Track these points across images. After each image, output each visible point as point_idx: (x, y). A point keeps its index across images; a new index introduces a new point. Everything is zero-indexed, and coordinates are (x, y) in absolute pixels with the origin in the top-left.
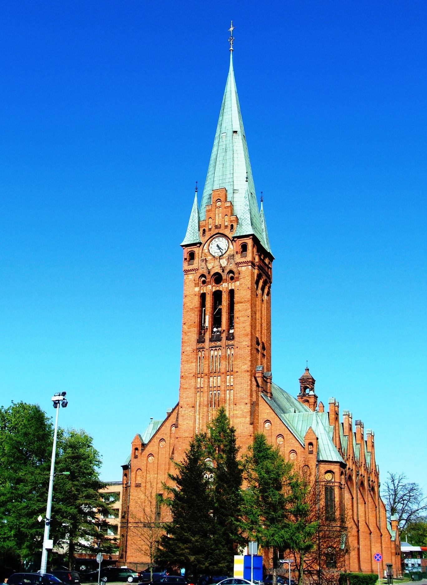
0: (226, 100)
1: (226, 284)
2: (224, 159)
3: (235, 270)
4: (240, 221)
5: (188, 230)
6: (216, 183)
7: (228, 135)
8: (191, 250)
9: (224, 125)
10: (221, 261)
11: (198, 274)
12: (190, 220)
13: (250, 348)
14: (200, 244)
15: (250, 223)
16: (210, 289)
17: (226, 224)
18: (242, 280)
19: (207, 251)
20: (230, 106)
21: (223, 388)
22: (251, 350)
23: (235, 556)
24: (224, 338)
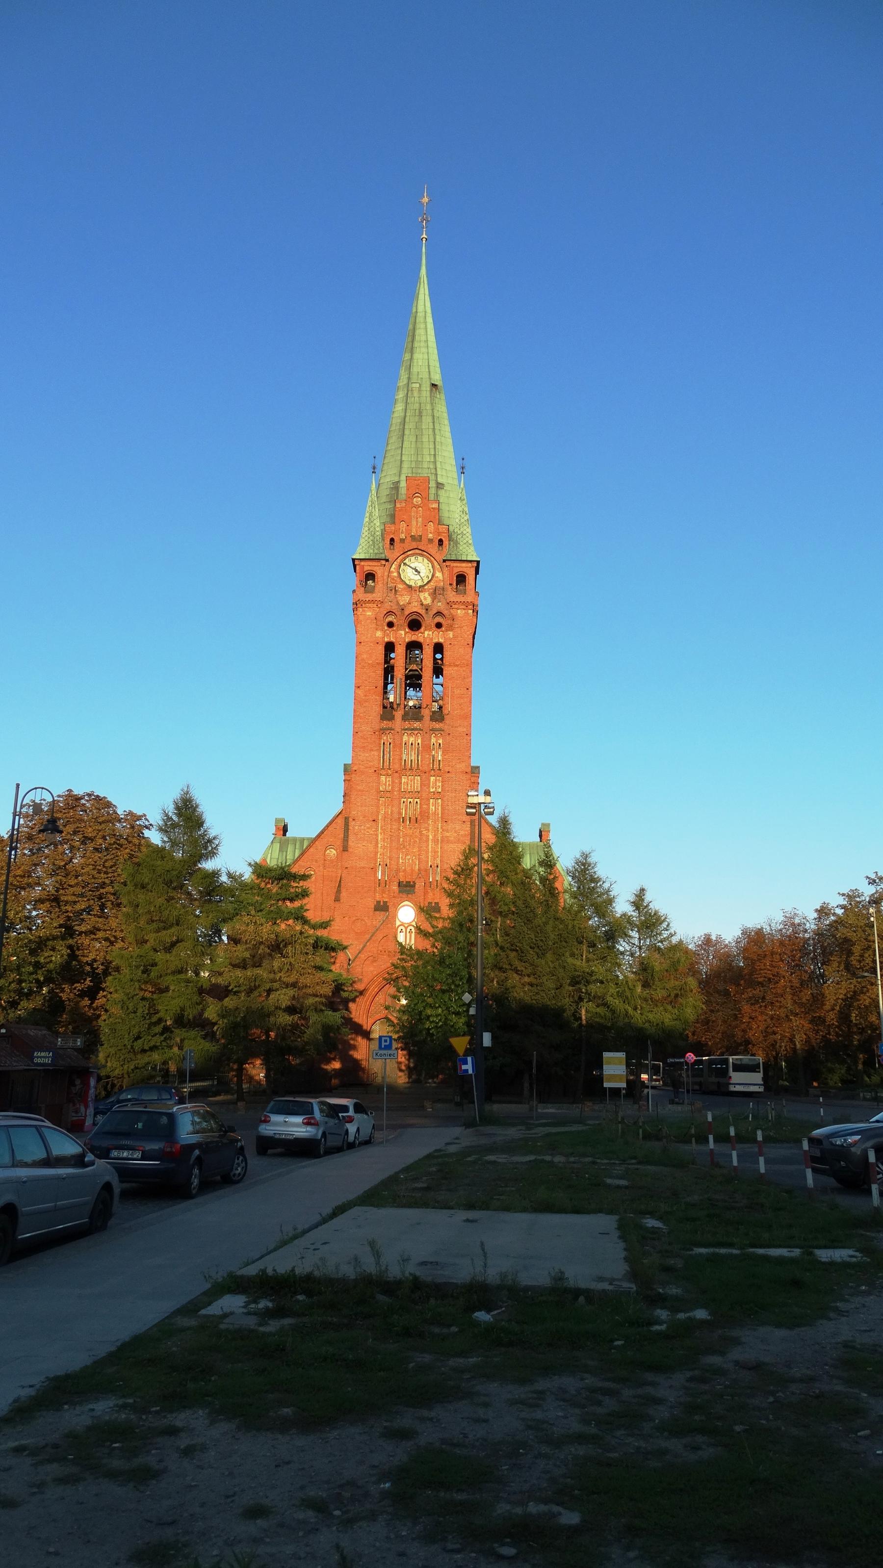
0: (418, 326)
2: (418, 427)
3: (445, 612)
4: (454, 536)
6: (405, 465)
7: (423, 388)
8: (369, 568)
9: (415, 370)
14: (387, 560)
17: (430, 536)
18: (458, 631)
19: (395, 574)
20: (423, 338)
21: (424, 795)
24: (427, 718)
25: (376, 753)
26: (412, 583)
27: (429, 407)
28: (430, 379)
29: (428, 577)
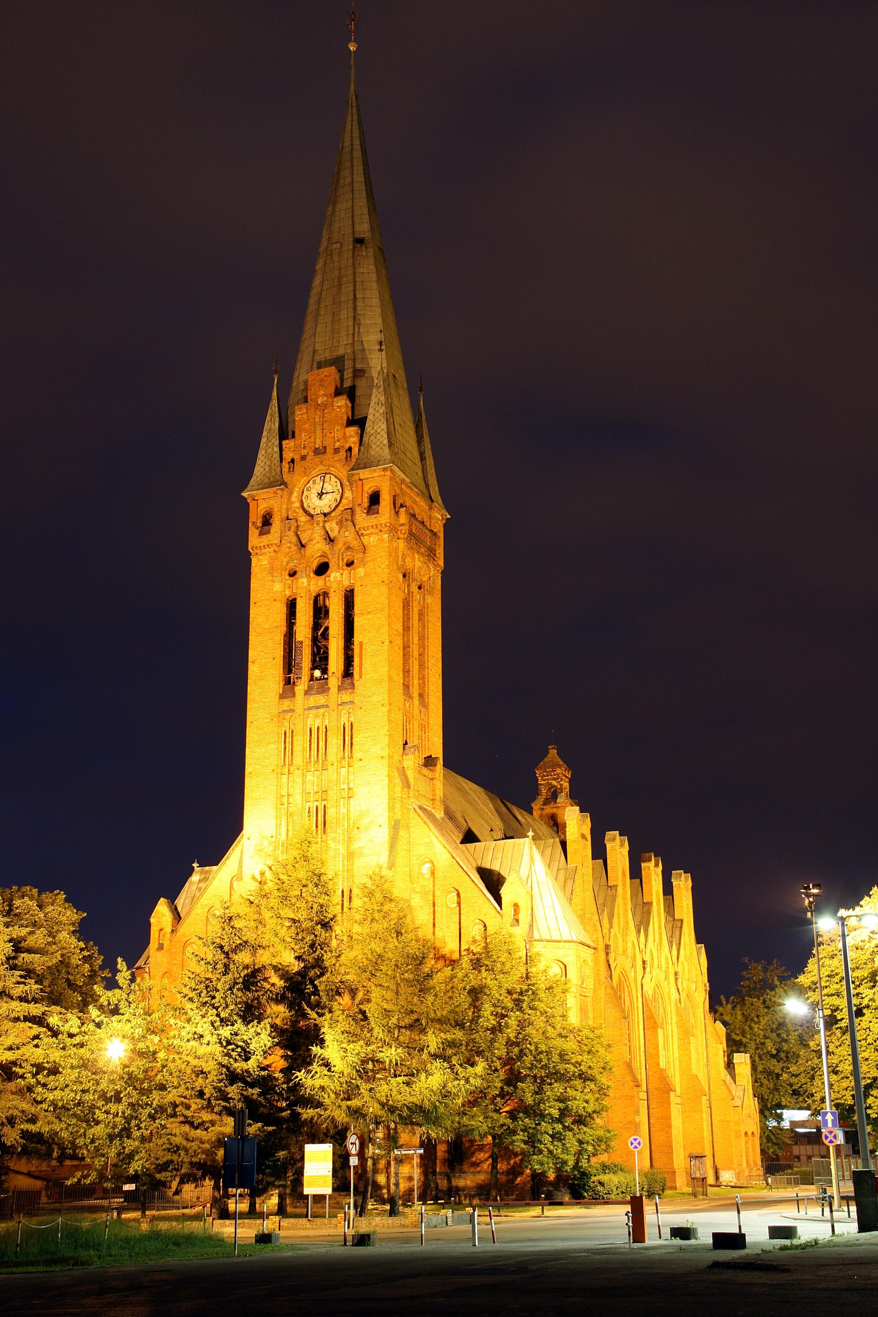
1: (338, 574)
3: (355, 543)
5: (259, 462)
10: (327, 525)
12: (264, 440)
13: (386, 709)
15: (386, 442)
16: (307, 586)
19: (297, 505)
20: (348, 180)
22: (389, 711)
23: (306, 1145)
25: (273, 746)
27: (350, 271)
28: (353, 232)
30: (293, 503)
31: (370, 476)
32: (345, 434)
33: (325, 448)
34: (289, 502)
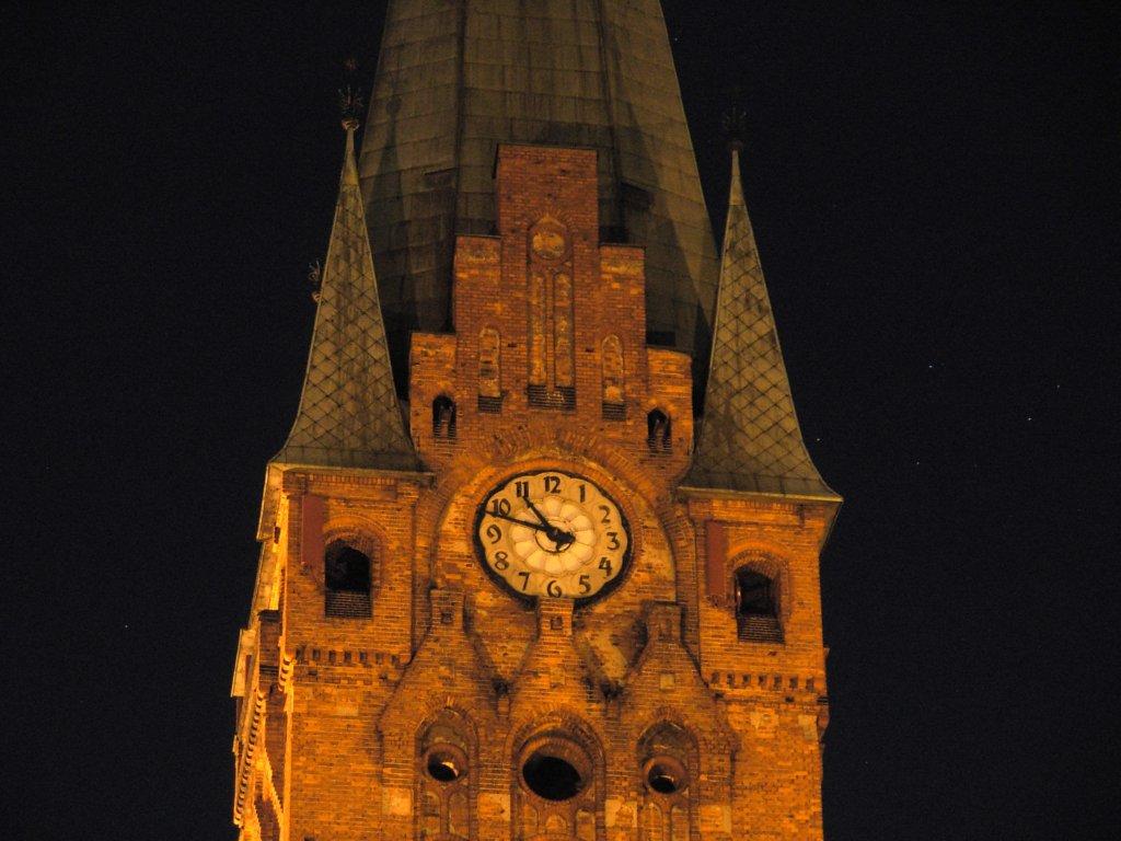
3: (698, 719)
4: (715, 398)
11: (406, 694)
18: (755, 804)
19: (462, 547)
26: (537, 586)
29: (605, 565)
30: (447, 538)
31: (743, 517)
32: (644, 364)
33: (570, 393)
34: (437, 537)
